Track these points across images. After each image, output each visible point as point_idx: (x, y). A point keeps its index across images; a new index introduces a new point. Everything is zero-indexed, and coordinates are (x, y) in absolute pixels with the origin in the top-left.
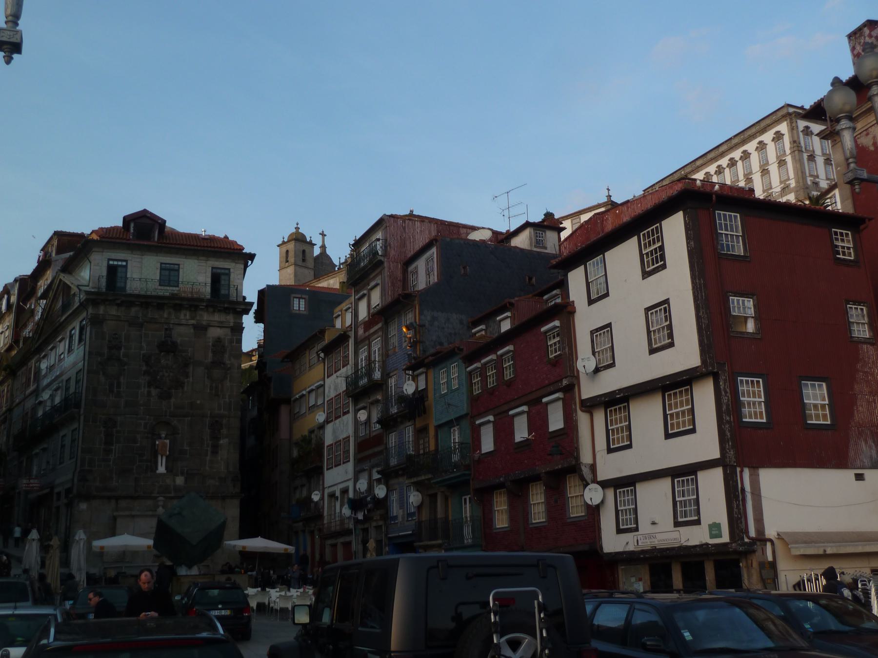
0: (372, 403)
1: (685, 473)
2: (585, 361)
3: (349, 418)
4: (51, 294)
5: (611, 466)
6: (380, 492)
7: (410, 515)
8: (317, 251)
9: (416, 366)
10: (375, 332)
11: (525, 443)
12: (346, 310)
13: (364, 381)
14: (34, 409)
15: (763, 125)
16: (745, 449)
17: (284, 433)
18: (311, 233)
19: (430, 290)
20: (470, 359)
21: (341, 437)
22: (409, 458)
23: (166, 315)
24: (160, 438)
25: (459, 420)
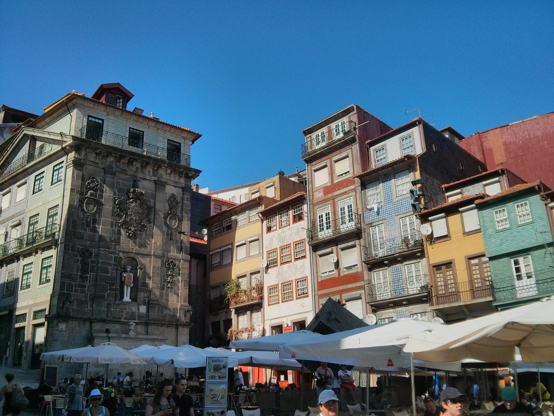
3: (306, 262)
12: (267, 188)
13: (325, 234)
21: (293, 278)
23: (134, 169)
24: (126, 271)
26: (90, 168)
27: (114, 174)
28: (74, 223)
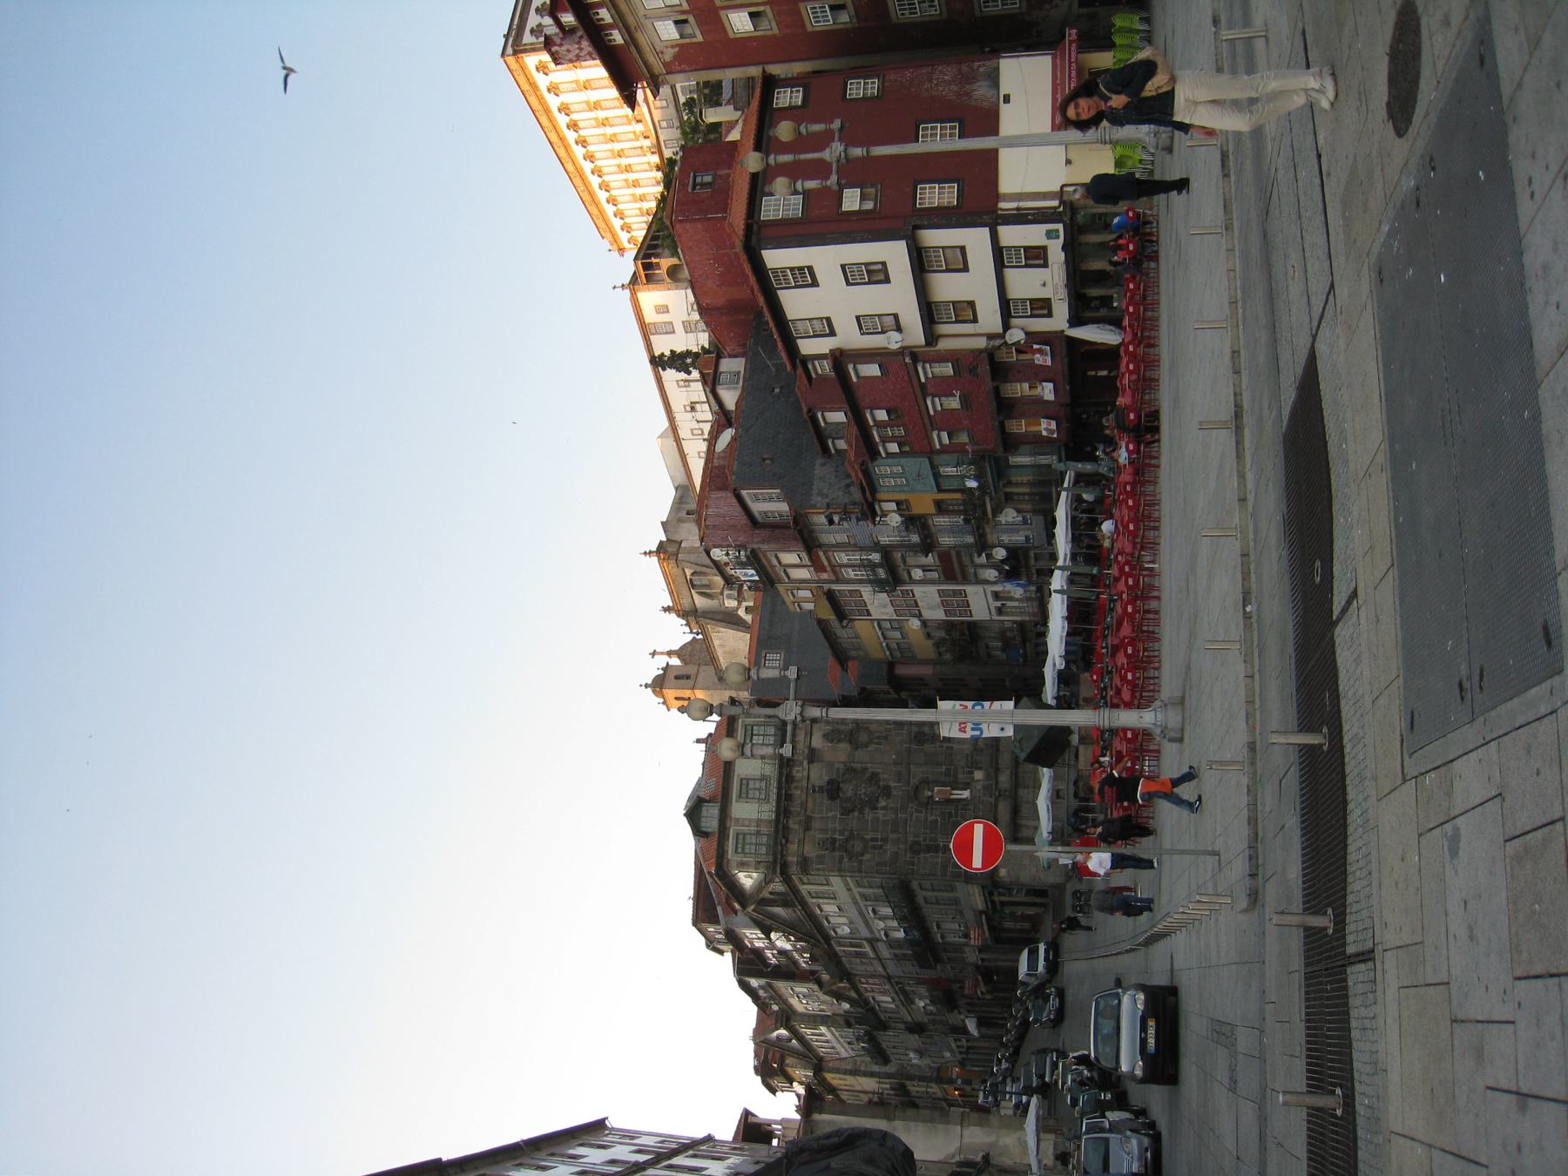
0: (904, 562)
1: (1000, 256)
2: (893, 341)
4: (768, 922)
5: (990, 318)
6: (1000, 553)
7: (1025, 522)
8: (675, 661)
9: (870, 512)
10: (828, 558)
11: (964, 400)
14: (892, 944)
15: (526, 87)
16: (980, 203)
17: (926, 671)
18: (654, 668)
19: (788, 497)
20: (873, 453)
22: (967, 521)
25: (933, 467)
26: (810, 851)
27: (809, 819)
28: (878, 864)
